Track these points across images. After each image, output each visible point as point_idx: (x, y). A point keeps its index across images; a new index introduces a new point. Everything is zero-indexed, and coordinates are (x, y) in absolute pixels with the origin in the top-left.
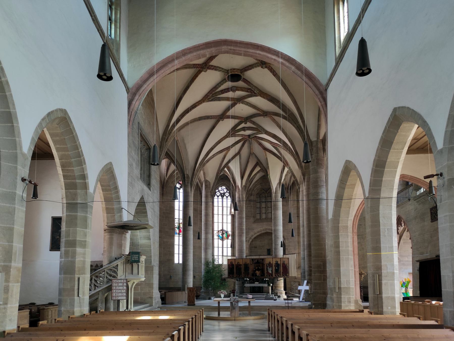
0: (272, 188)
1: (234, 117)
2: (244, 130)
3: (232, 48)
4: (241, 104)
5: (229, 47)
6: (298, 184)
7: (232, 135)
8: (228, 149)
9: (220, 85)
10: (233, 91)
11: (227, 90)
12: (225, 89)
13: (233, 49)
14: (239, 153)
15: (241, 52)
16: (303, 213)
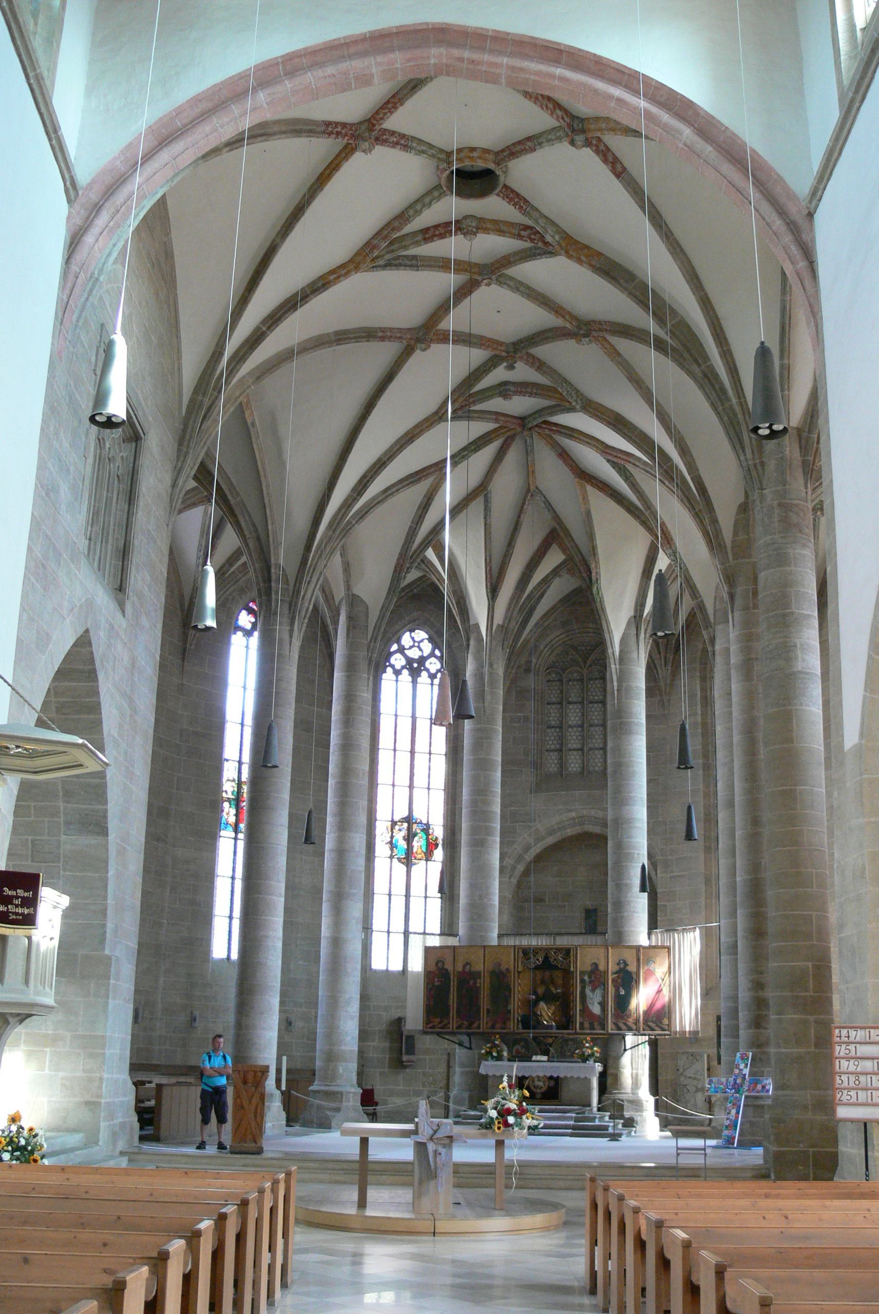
0: (607, 636)
1: (465, 339)
4: (494, 287)
5: (456, 52)
6: (708, 625)
7: (460, 413)
9: (418, 207)
10: (465, 234)
12: (436, 227)
13: (468, 59)
15: (497, 71)
16: (730, 746)
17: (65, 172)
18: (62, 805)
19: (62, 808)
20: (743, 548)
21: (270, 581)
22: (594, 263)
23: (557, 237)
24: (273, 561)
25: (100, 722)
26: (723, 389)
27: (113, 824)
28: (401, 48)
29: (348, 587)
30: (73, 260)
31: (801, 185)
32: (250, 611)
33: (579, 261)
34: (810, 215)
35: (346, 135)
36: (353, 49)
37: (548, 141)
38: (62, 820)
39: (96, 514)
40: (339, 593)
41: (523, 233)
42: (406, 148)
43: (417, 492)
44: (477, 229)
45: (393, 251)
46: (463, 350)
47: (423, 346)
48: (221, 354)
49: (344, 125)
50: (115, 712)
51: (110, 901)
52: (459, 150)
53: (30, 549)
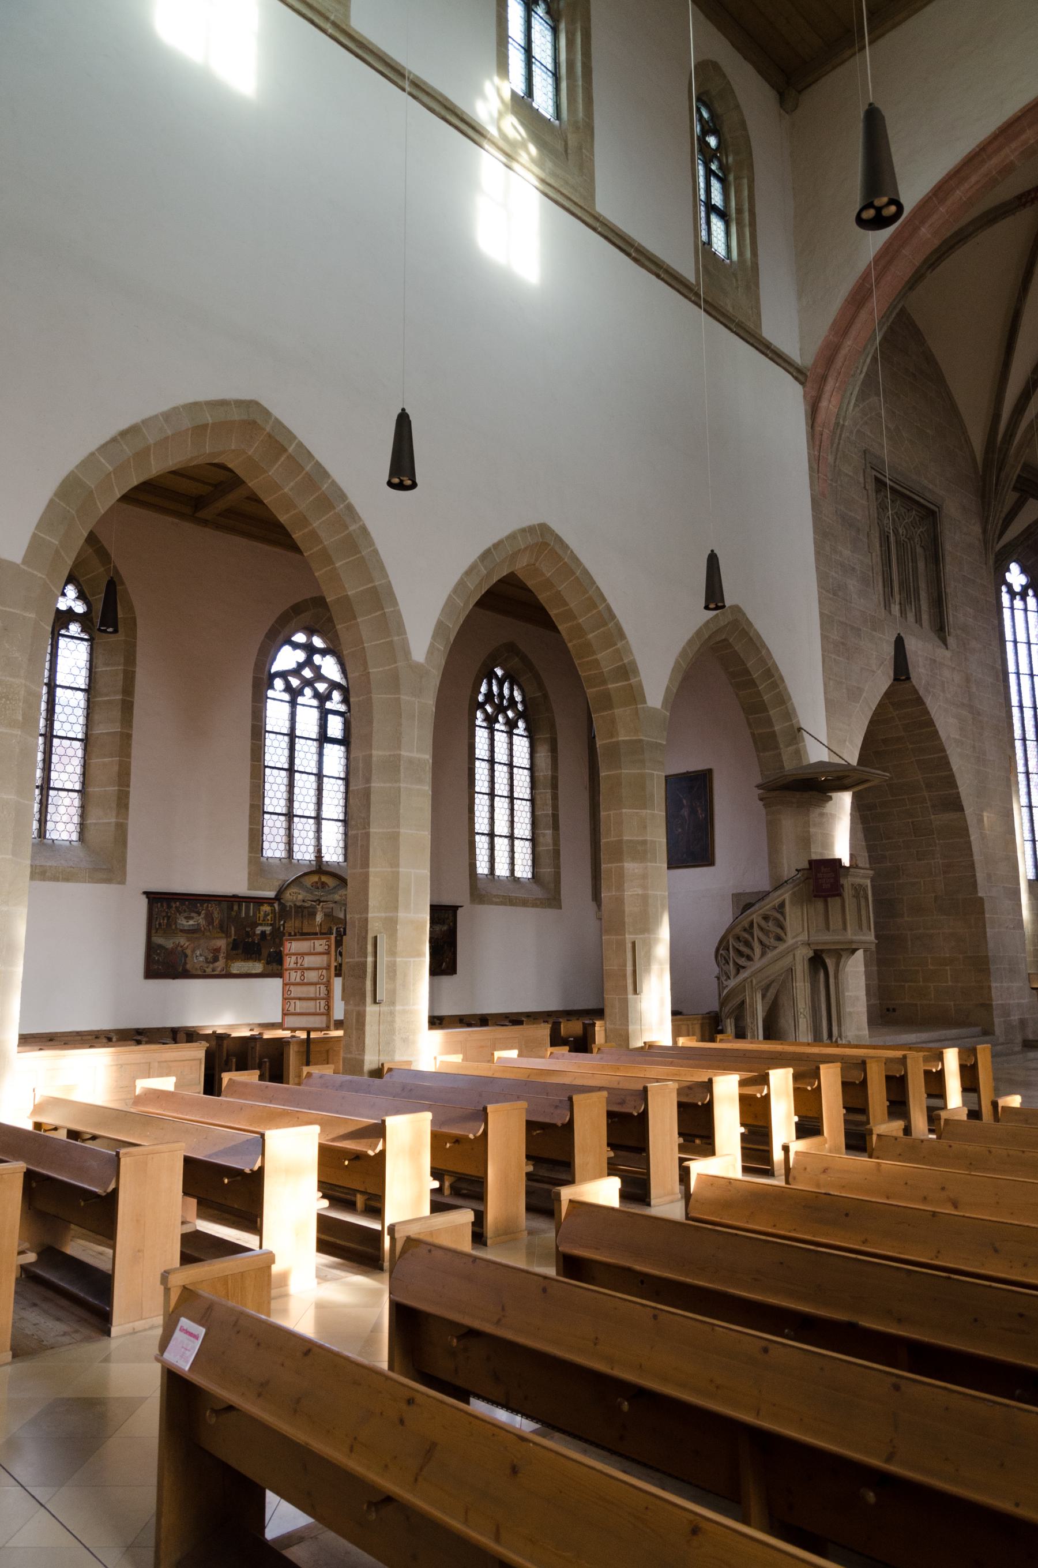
18: (926, 794)
19: (927, 796)
25: (937, 732)
38: (929, 804)
51: (977, 857)
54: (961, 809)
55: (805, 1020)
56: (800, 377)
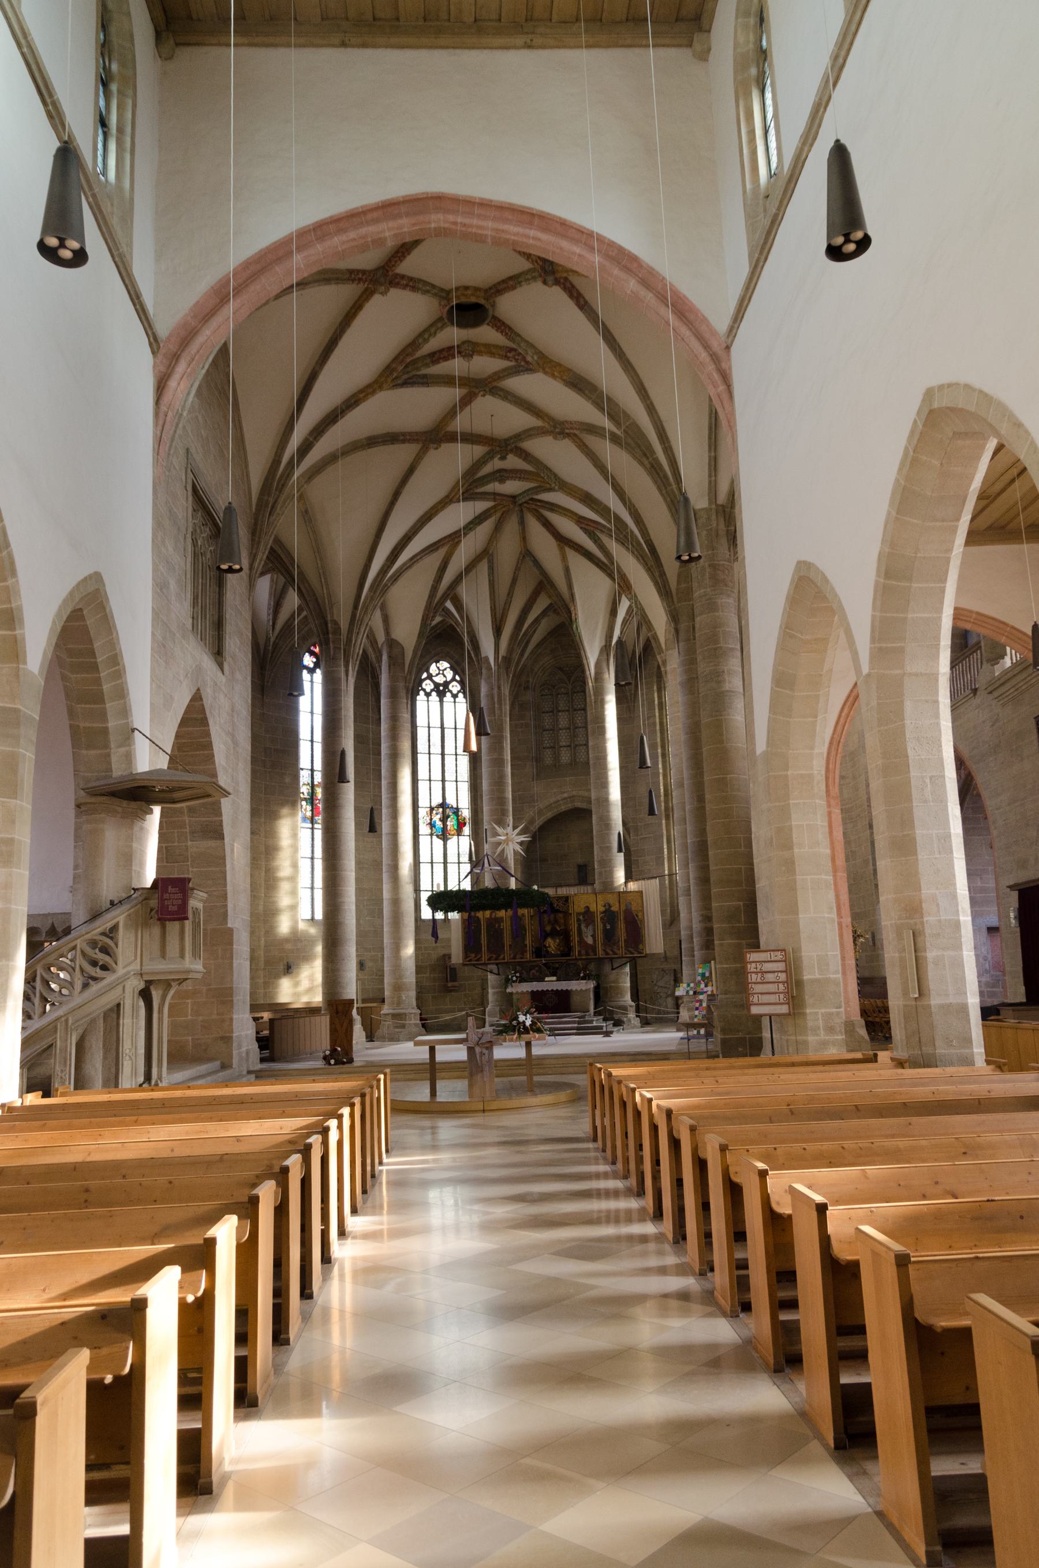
0: (585, 662)
1: (470, 438)
2: (502, 481)
3: (459, 220)
4: (488, 397)
5: (451, 218)
6: (661, 651)
7: (466, 495)
8: (453, 539)
9: (426, 336)
10: (464, 357)
11: (446, 353)
12: (441, 351)
13: (461, 223)
14: (486, 554)
15: (485, 232)
17: (148, 330)
18: (187, 819)
20: (687, 594)
21: (328, 633)
22: (565, 378)
23: (536, 358)
24: (329, 618)
26: (666, 476)
27: (227, 830)
28: (407, 215)
29: (387, 632)
30: (161, 402)
31: (721, 323)
32: (312, 653)
33: (553, 376)
34: (728, 348)
35: (366, 281)
36: (369, 216)
37: (527, 280)
39: (195, 598)
40: (381, 638)
41: (509, 354)
42: (414, 289)
43: (434, 561)
44: (473, 352)
45: (408, 372)
46: (468, 447)
47: (435, 446)
48: (279, 462)
49: (364, 272)
50: (222, 746)
51: (229, 888)
52: (457, 289)
53: (153, 634)
54: (221, 836)
55: (130, 1062)
56: (154, 345)
